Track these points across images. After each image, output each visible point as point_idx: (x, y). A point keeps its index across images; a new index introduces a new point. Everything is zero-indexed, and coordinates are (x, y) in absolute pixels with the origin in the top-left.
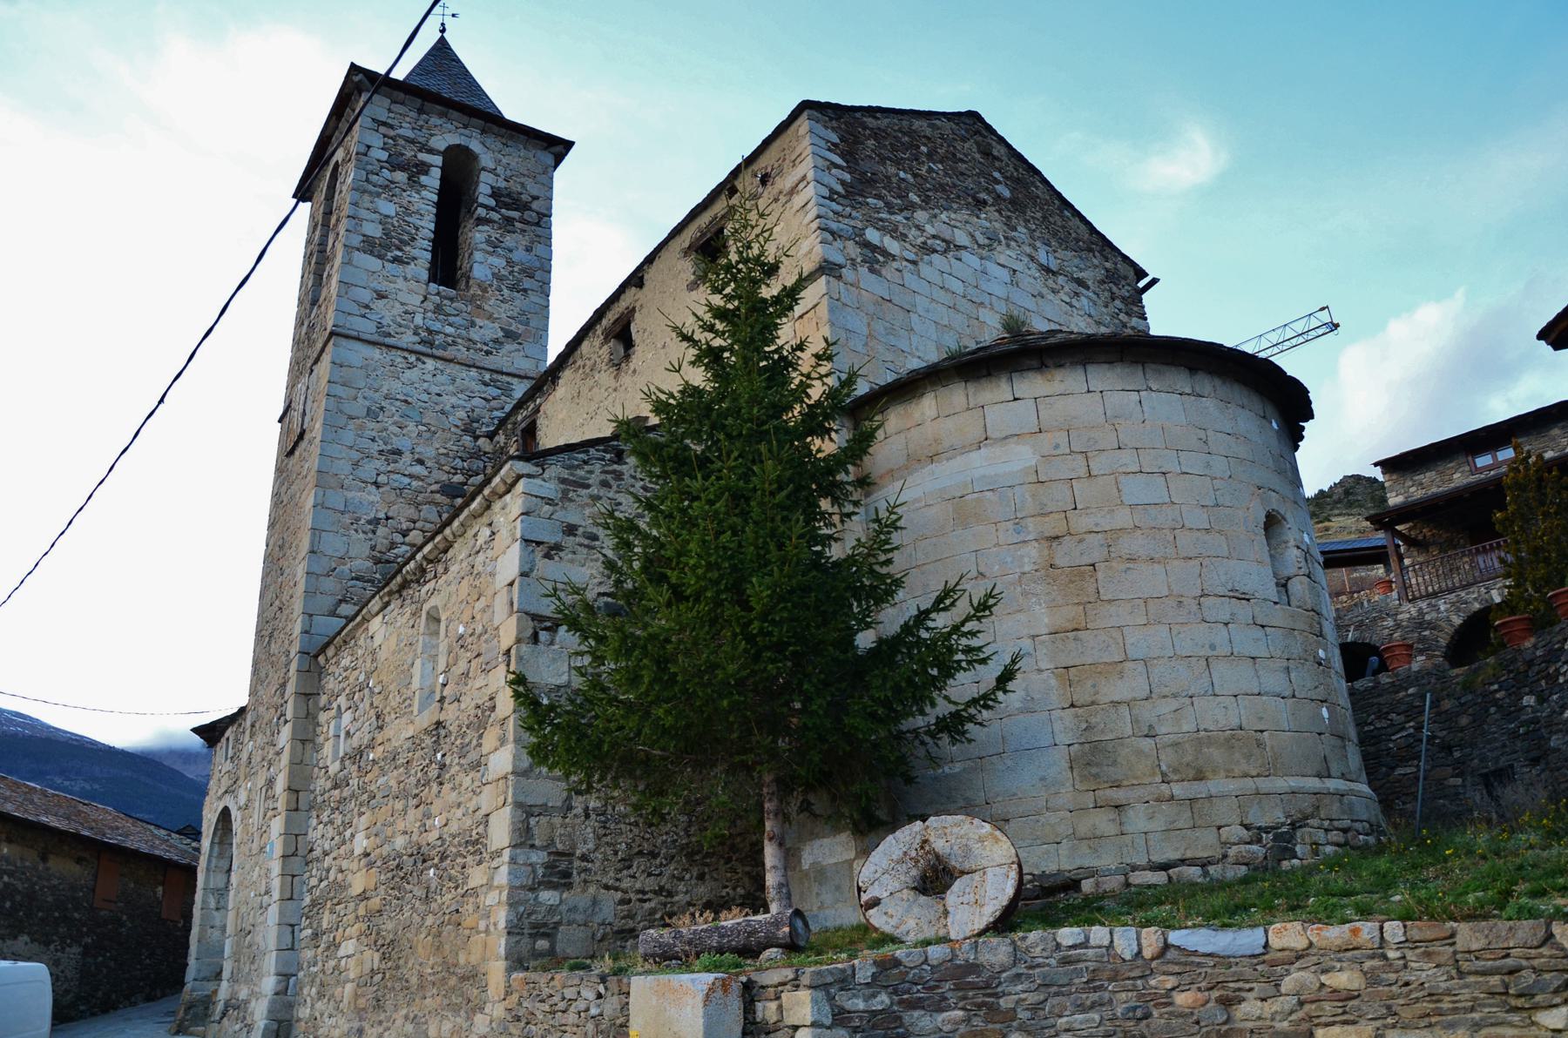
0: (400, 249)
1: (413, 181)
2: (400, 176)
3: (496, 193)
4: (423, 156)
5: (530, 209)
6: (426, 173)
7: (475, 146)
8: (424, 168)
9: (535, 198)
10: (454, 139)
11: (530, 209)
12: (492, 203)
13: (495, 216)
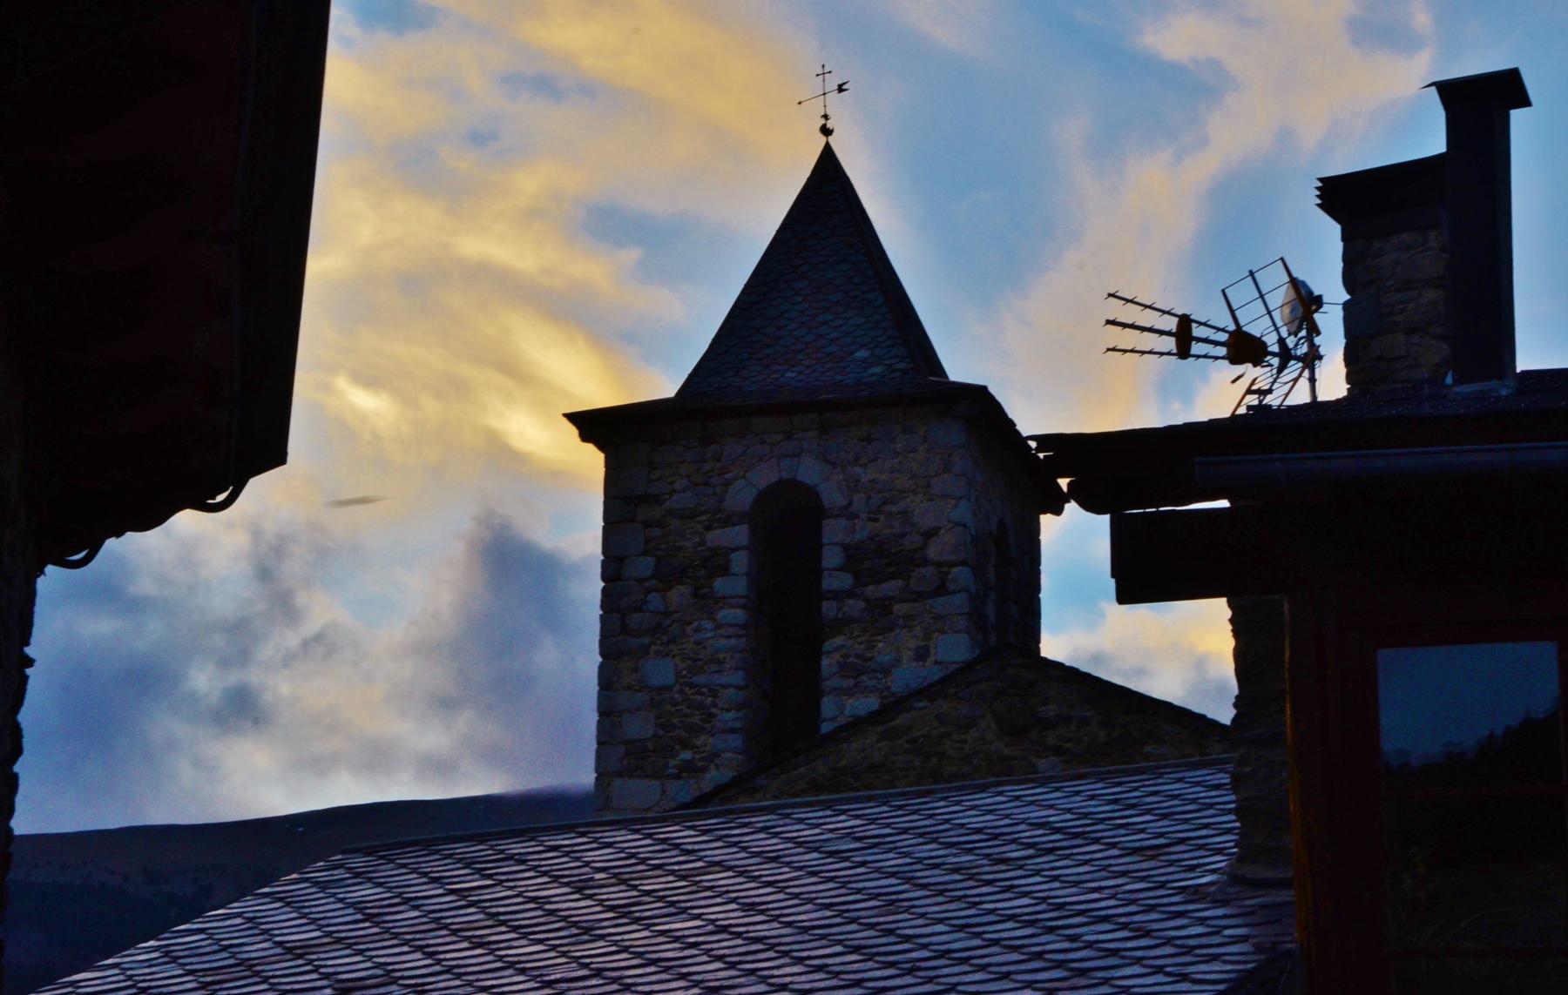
0: (687, 746)
1: (706, 602)
2: (679, 595)
3: (853, 557)
4: (719, 537)
5: (926, 562)
6: (725, 571)
7: (809, 471)
8: (717, 563)
9: (930, 534)
10: (764, 476)
11: (926, 562)
12: (843, 581)
13: (854, 607)
